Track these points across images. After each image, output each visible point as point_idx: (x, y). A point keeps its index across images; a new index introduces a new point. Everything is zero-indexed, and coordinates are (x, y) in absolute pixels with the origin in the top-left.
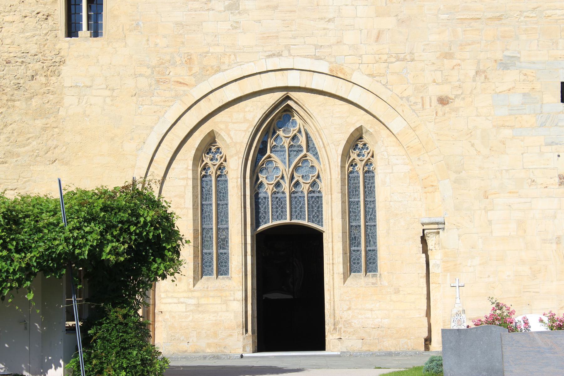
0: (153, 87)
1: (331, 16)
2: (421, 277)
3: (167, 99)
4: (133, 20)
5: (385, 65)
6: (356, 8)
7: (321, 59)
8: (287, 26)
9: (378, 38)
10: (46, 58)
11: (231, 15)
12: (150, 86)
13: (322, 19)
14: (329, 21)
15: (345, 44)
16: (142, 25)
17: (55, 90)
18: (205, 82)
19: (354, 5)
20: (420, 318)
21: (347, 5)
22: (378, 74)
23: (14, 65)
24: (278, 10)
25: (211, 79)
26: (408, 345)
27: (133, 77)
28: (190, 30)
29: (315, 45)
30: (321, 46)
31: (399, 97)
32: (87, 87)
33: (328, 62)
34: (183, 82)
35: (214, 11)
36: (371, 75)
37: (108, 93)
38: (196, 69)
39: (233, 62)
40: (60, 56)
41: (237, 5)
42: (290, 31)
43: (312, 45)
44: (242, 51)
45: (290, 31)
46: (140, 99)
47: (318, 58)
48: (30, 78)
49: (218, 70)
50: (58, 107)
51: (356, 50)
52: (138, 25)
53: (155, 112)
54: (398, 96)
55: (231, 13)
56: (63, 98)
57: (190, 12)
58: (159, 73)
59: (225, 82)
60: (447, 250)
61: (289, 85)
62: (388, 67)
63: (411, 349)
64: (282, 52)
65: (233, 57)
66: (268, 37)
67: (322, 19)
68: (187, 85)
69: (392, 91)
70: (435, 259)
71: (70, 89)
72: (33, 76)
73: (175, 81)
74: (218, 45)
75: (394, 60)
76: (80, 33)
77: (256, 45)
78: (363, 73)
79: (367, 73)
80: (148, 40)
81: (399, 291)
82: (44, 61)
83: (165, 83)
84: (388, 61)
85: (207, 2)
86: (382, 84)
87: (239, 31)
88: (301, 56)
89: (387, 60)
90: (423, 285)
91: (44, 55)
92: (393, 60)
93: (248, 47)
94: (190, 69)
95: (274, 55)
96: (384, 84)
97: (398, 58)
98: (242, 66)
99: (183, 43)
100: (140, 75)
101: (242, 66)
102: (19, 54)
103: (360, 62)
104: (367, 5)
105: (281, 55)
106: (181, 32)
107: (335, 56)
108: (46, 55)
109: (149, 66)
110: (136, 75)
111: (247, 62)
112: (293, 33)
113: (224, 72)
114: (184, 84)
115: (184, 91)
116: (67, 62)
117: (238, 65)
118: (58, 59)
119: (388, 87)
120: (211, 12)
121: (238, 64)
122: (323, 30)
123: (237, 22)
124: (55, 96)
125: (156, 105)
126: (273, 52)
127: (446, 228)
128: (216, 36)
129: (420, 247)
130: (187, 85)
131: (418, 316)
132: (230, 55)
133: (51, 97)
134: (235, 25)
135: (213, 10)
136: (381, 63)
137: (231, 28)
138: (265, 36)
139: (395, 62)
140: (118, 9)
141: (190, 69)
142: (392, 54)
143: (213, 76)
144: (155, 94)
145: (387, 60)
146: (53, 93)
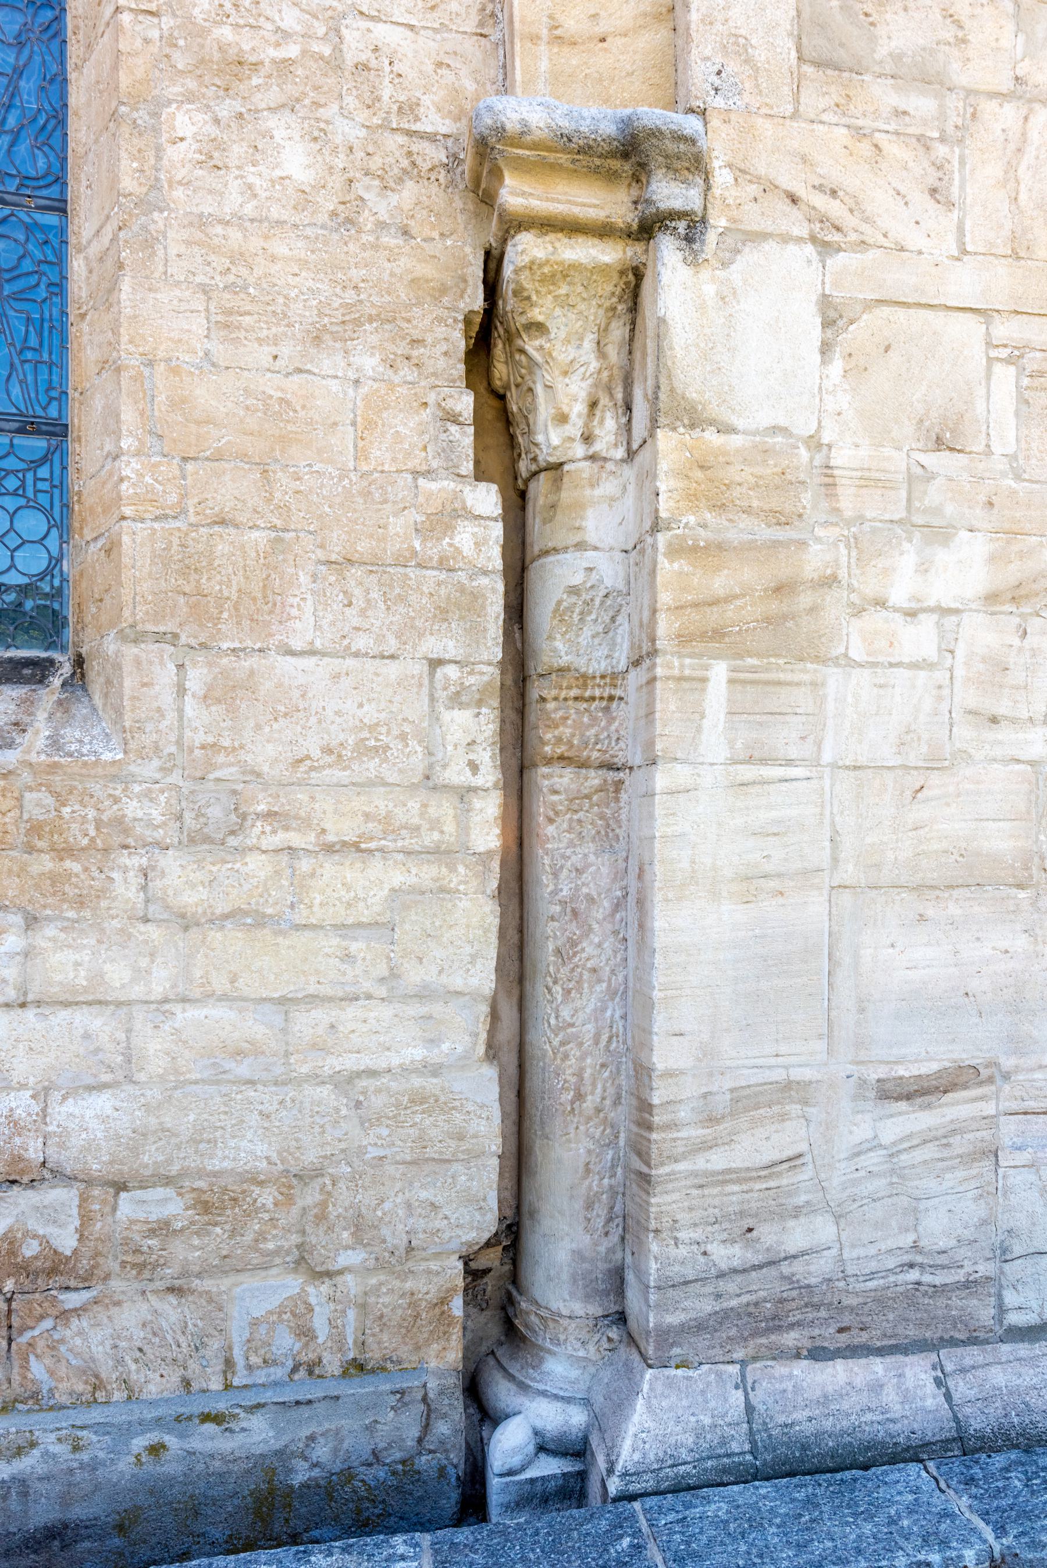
2: (456, 700)
20: (435, 1070)
26: (306, 1333)
60: (710, 436)
63: (332, 1364)
70: (581, 546)
81: (244, 817)
90: (474, 767)
127: (718, 221)
129: (453, 418)
131: (417, 1053)
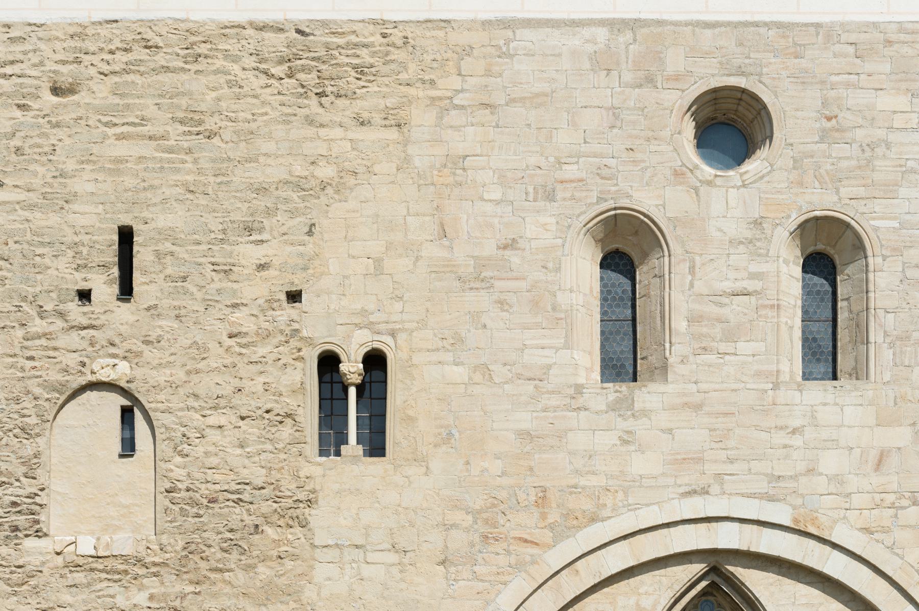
0: (477, 548)
1: (797, 423)
3: (501, 570)
4: (442, 427)
5: (892, 512)
6: (842, 410)
7: (778, 500)
8: (719, 440)
9: (879, 465)
10: (280, 493)
11: (619, 419)
12: (472, 545)
13: (781, 428)
14: (794, 432)
15: (821, 474)
16: (457, 435)
17: (297, 551)
18: (571, 539)
19: (837, 404)
21: (825, 404)
22: (879, 529)
23: (222, 505)
24: (703, 412)
25: (580, 535)
27: (441, 530)
28: (544, 446)
29: (766, 475)
30: (779, 477)
31: (915, 570)
32: (357, 547)
33: (791, 505)
34: (529, 538)
35: (587, 412)
36: (867, 530)
37: (392, 558)
38: (554, 516)
39: (620, 504)
40: (307, 491)
41: (630, 401)
42: (724, 449)
43: (764, 474)
44: (638, 484)
45: (724, 449)
46: (452, 569)
47: (772, 499)
48: (252, 530)
49: (594, 519)
50: (302, 583)
51: (841, 485)
52: (450, 434)
53: (478, 593)
54: (913, 567)
55: (620, 415)
56: (312, 567)
57: (545, 413)
58: (487, 523)
59: (607, 540)
61: (720, 547)
62: (896, 516)
64: (709, 486)
65: (620, 495)
66: (684, 459)
67: (781, 428)
68: (536, 544)
69: (902, 559)
71: (325, 550)
72: (257, 526)
73: (515, 538)
74: (594, 473)
75: (905, 503)
76: (343, 448)
77: (663, 474)
78: (852, 526)
79: (859, 526)
80: (468, 463)
82: (277, 499)
83: (497, 540)
84: (897, 505)
85: (574, 395)
86: (885, 546)
87: (633, 448)
88: (743, 495)
89: (894, 503)
91: (278, 488)
92: (905, 503)
93: (649, 478)
94: (544, 516)
95: (695, 492)
96: (889, 545)
97: (913, 500)
98: (637, 512)
99: (531, 469)
100: (454, 526)
101: (638, 511)
102: (234, 487)
103: (847, 506)
104: (861, 405)
105: (707, 493)
106: (528, 448)
107: (803, 496)
108: (282, 489)
109: (470, 510)
110: (445, 525)
111: (647, 505)
112: (729, 452)
113: (605, 523)
114: (532, 542)
115: (532, 556)
116: (321, 502)
117: (631, 510)
118: (302, 496)
119: (897, 551)
120: (582, 413)
121: (629, 508)
122: (784, 448)
123: (628, 432)
124: (299, 562)
125: (482, 581)
126: (693, 487)
128: (590, 456)
130: (536, 544)
132: (617, 492)
133: (289, 564)
134: (625, 437)
135: (586, 410)
136: (885, 508)
137: (618, 443)
138: (679, 457)
139: (908, 507)
140: (414, 405)
141: (544, 516)
142: (904, 493)
143: (585, 530)
144: (480, 561)
145: (894, 503)
146: (294, 557)
